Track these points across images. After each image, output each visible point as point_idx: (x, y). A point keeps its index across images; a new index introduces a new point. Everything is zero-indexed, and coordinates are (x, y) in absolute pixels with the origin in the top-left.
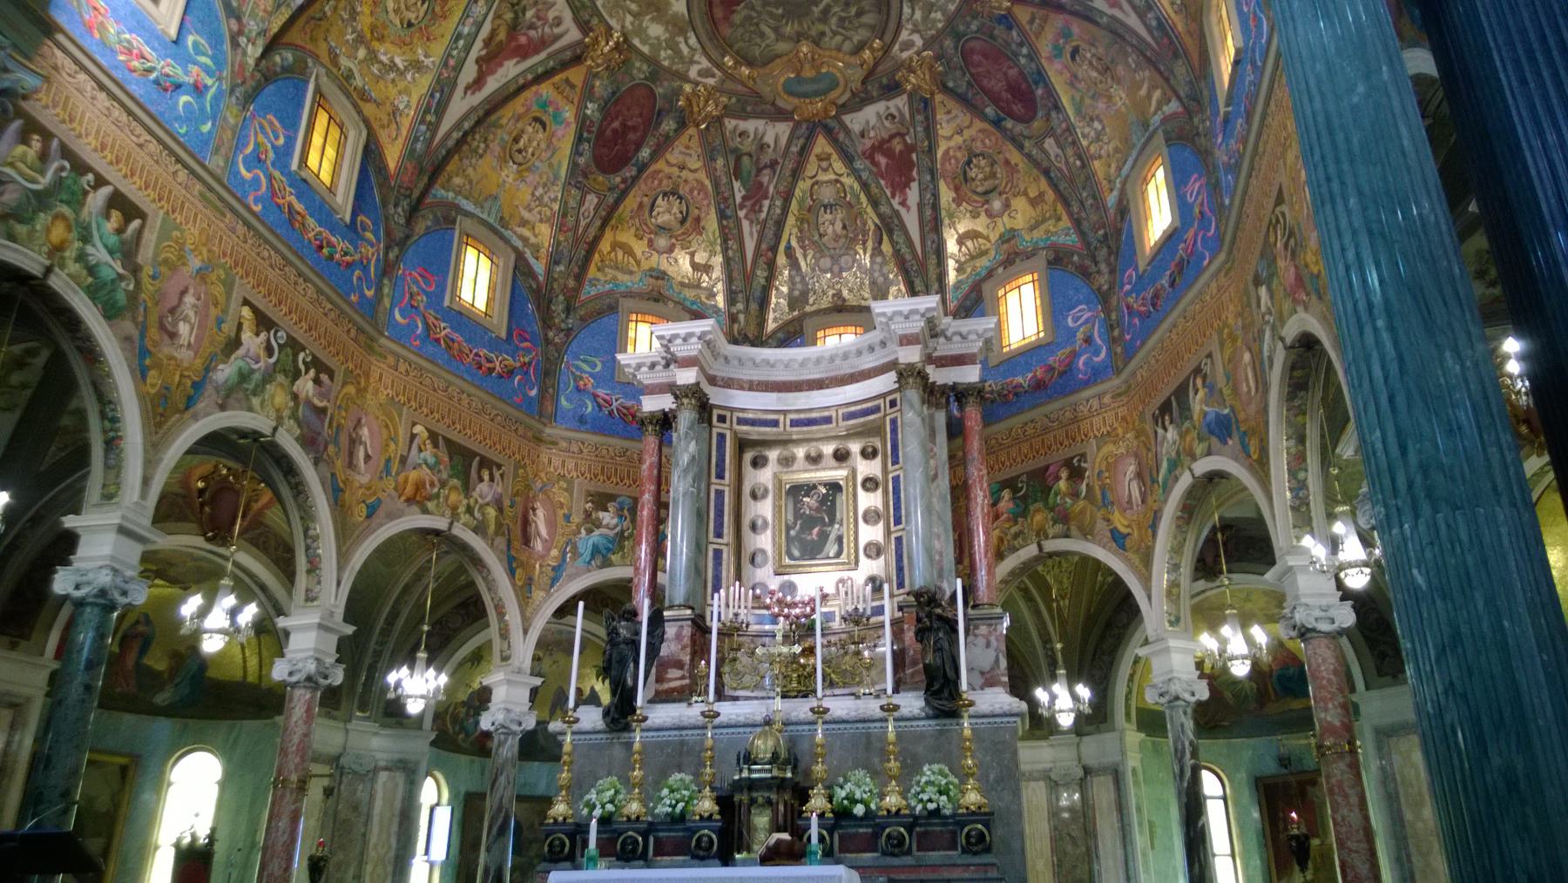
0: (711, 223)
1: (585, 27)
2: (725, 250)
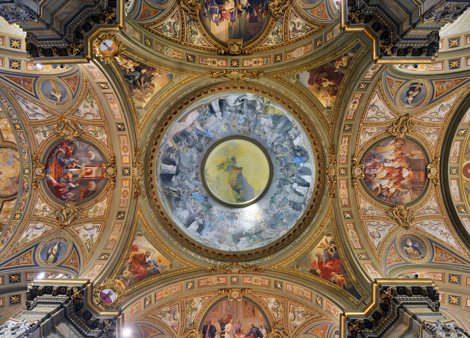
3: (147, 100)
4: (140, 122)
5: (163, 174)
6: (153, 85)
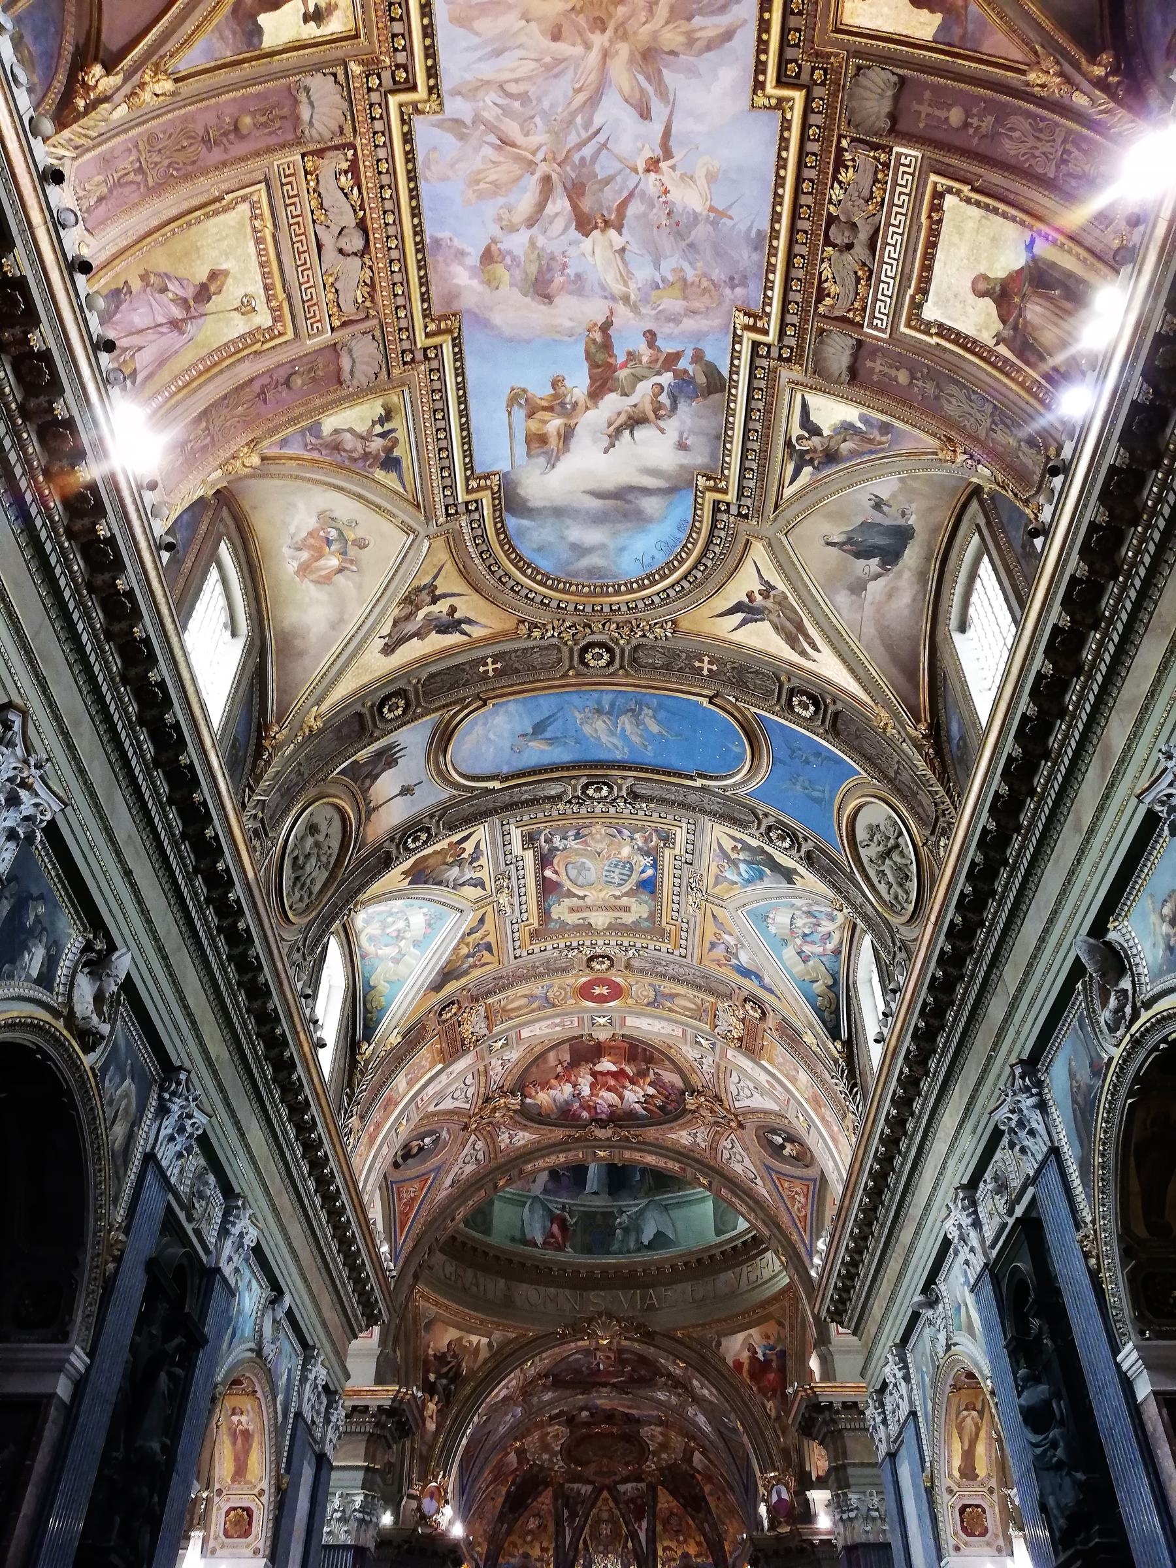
0: (551, 1528)
1: (520, 1462)
2: (556, 1540)
3: (474, 1339)
6: (450, 1344)
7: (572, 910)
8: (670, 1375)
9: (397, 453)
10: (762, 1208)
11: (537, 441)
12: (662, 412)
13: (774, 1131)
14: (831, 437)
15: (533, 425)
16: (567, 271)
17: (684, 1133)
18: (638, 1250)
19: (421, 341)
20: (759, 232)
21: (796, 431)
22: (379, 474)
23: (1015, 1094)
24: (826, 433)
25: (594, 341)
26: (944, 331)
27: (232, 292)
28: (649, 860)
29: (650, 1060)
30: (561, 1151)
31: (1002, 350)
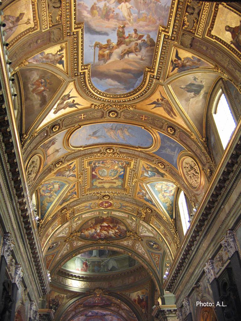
3: (63, 295)
4: (73, 294)
5: (99, 253)
6: (56, 296)
7: (99, 183)
8: (115, 303)
9: (63, 59)
10: (146, 261)
11: (101, 57)
12: (137, 50)
13: (151, 242)
14: (184, 61)
15: (101, 52)
16: (114, 12)
17: (125, 242)
18: (107, 271)
19: (74, 30)
20: (168, 7)
21: (174, 58)
22: (58, 65)
23: (227, 237)
24: (183, 60)
25: (120, 31)
26: (217, 38)
27: (25, 19)
28: (122, 170)
29: (117, 223)
30: (91, 247)
31: (232, 45)
